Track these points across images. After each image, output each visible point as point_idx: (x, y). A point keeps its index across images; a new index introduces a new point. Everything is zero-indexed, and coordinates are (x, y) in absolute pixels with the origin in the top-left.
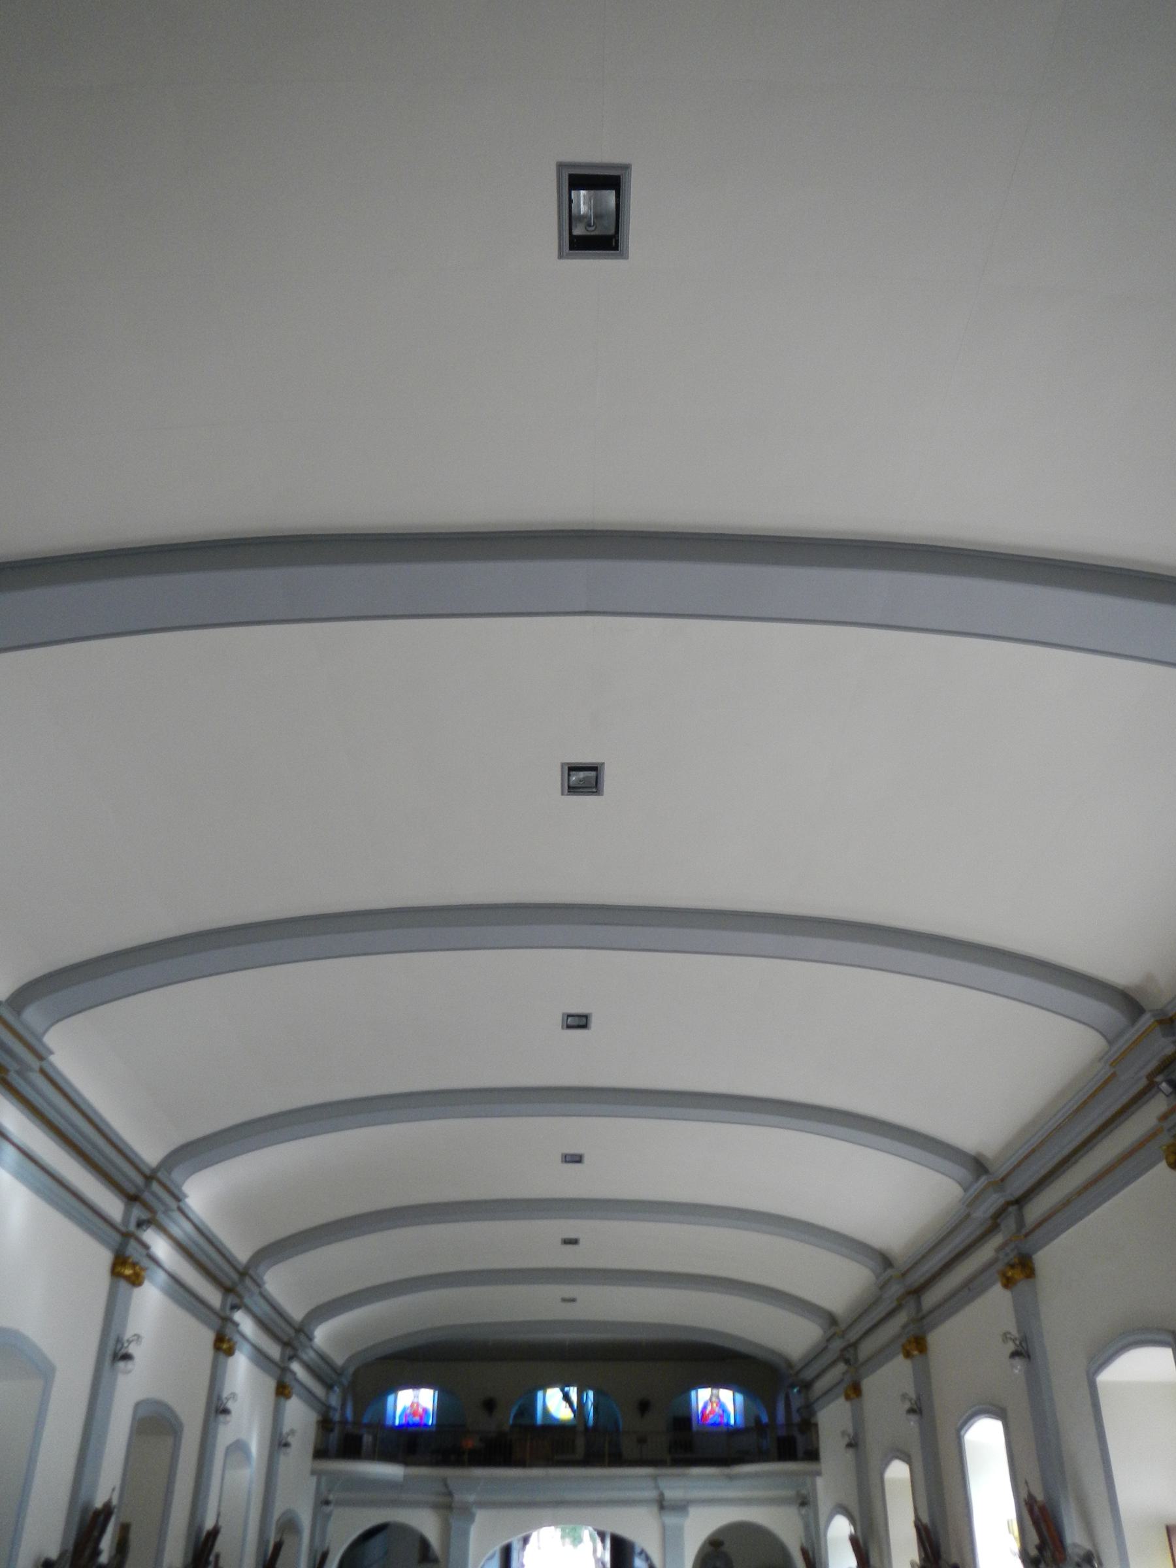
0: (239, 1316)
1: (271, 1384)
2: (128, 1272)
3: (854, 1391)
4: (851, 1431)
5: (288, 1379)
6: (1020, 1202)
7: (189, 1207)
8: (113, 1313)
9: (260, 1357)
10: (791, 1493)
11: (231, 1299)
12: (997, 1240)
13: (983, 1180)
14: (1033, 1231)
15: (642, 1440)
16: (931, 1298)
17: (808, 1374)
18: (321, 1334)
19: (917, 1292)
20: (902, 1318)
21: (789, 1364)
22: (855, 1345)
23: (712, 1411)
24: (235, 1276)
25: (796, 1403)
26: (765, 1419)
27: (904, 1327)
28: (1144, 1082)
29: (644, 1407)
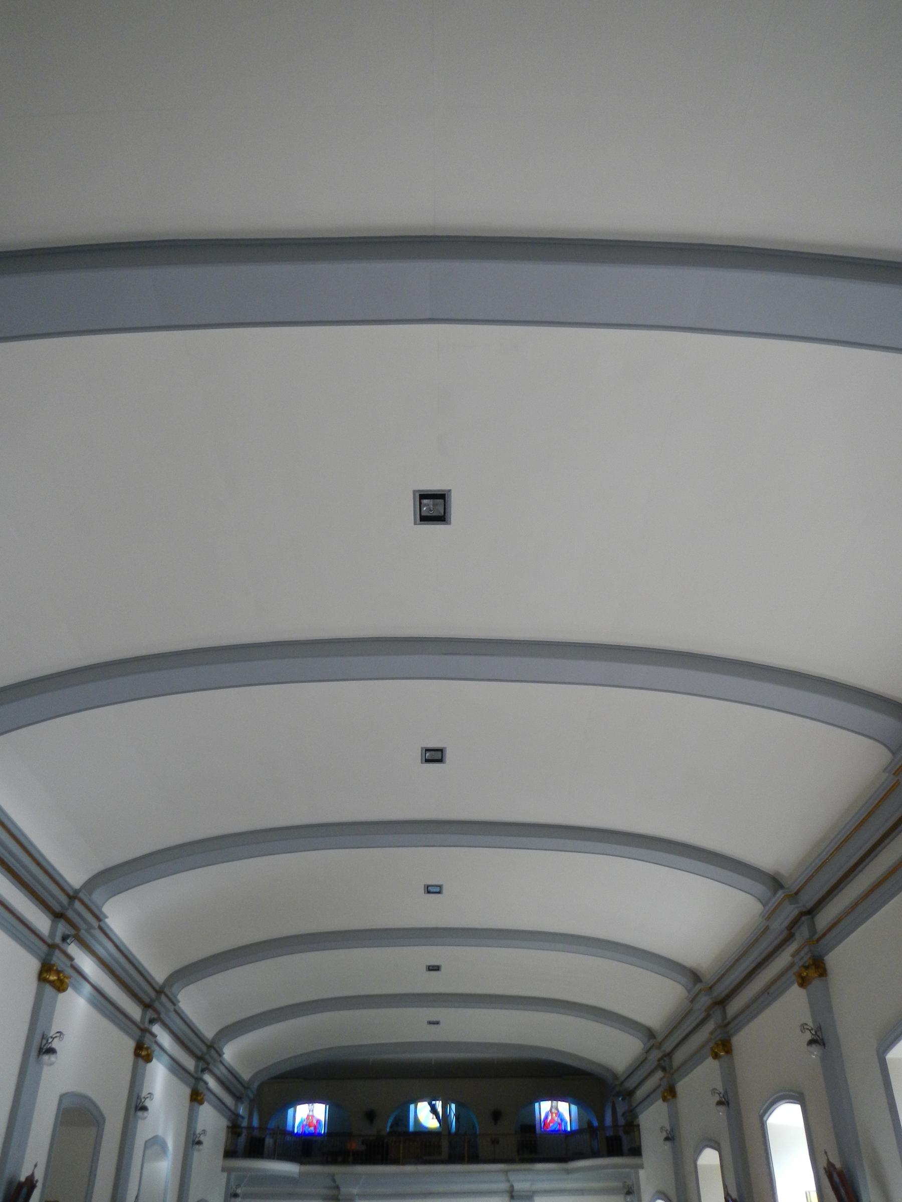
0: (157, 1029)
1: (187, 1091)
2: (53, 978)
3: (670, 1093)
5: (201, 1087)
6: (811, 912)
7: (108, 926)
9: (176, 1068)
11: (150, 1014)
12: (793, 947)
13: (780, 894)
14: (824, 935)
15: (495, 1142)
16: (734, 1007)
17: (630, 1085)
18: (230, 1052)
19: (722, 1003)
20: (710, 1025)
21: (615, 1076)
22: (669, 1055)
23: (552, 1120)
24: (153, 994)
25: (621, 1108)
26: (596, 1123)
27: (712, 1033)
29: (497, 1116)
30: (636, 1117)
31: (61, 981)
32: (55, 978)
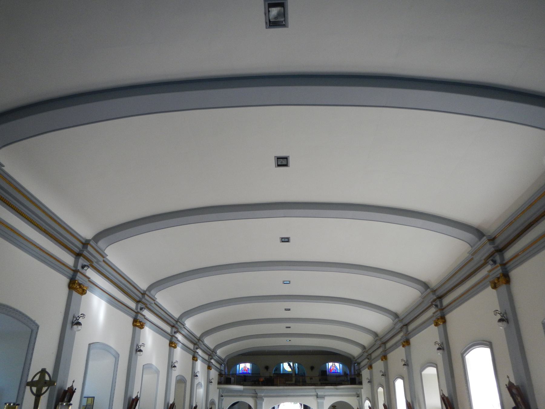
1: (206, 366)
2: (173, 345)
3: (370, 367)
4: (369, 378)
5: (211, 365)
6: (407, 325)
8: (170, 355)
10: (354, 393)
11: (196, 346)
12: (402, 334)
14: (411, 332)
15: (311, 379)
17: (359, 361)
18: (219, 352)
19: (385, 343)
20: (381, 350)
21: (354, 358)
22: (370, 354)
23: (333, 369)
24: (197, 341)
25: (357, 368)
26: (348, 372)
27: (381, 352)
28: (430, 303)
29: (312, 368)
30: (361, 372)
31: (175, 346)
32: (174, 345)
